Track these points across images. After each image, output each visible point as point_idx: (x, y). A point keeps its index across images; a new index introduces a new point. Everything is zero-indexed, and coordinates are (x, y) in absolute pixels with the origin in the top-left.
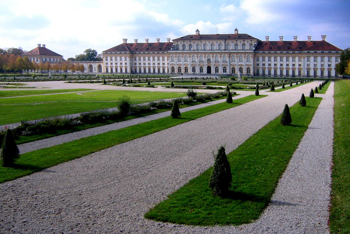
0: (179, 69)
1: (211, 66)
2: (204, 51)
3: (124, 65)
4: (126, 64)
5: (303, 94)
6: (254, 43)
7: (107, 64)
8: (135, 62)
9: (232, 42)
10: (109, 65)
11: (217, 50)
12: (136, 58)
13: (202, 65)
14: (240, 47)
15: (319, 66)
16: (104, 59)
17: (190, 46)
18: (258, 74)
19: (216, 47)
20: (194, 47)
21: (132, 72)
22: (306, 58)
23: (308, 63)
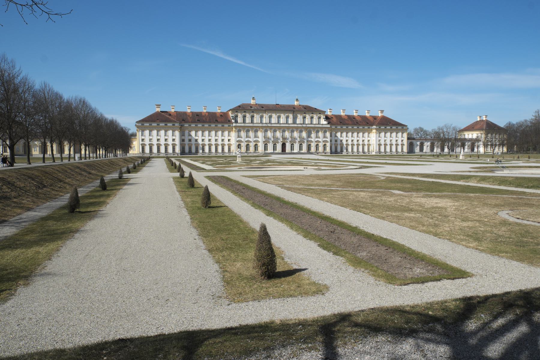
0: (248, 147)
1: (286, 144)
2: (278, 125)
3: (170, 142)
4: (174, 140)
5: (204, 177)
6: (323, 117)
7: (143, 140)
8: (183, 137)
9: (300, 116)
10: (147, 142)
11: (284, 124)
12: (184, 132)
13: (276, 142)
14: (308, 121)
15: (388, 142)
16: (139, 134)
17: (252, 117)
18: (391, 152)
19: (283, 120)
20: (257, 119)
21: (183, 152)
22: (378, 134)
23: (380, 138)
